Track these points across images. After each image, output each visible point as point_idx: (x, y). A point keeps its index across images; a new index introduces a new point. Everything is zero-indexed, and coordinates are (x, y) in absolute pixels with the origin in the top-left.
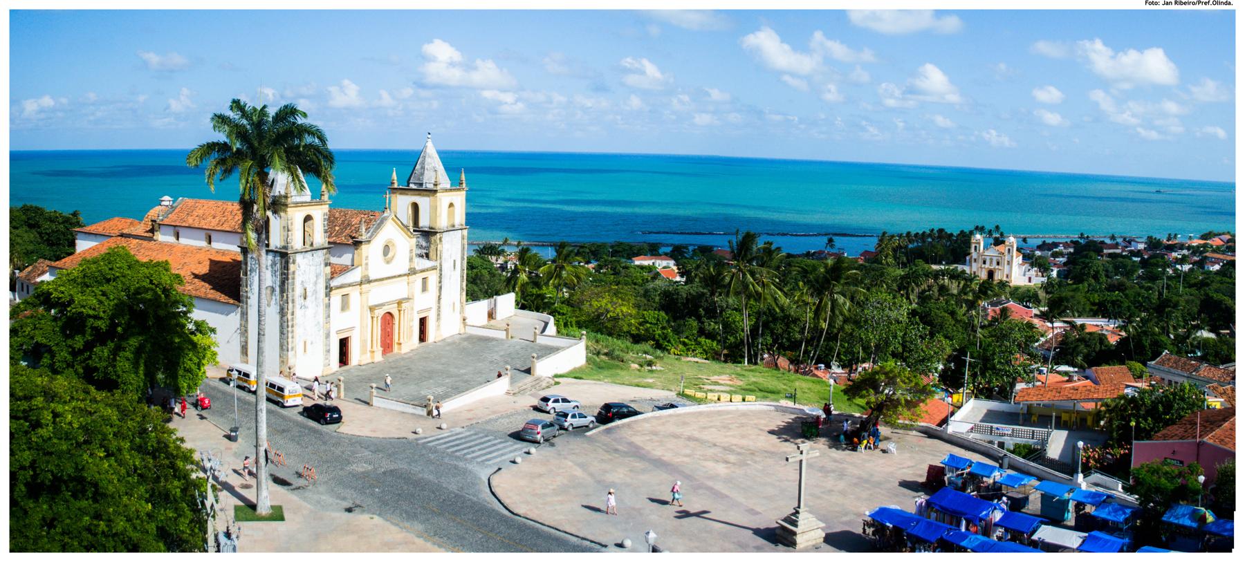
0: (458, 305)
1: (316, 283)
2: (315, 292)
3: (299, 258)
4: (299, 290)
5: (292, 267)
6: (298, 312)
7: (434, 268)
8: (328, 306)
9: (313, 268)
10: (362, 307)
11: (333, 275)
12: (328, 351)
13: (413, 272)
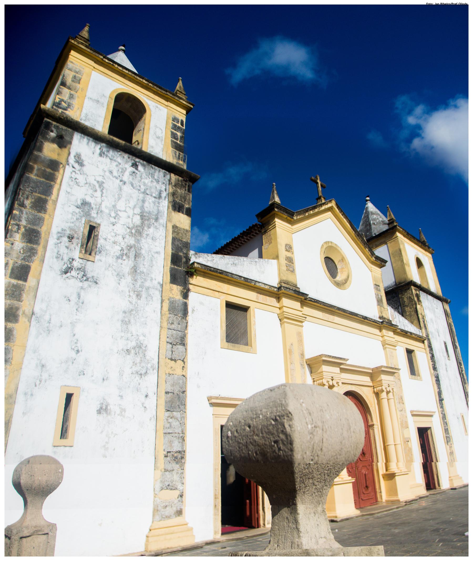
1: (138, 232)
2: (133, 252)
9: (127, 189)
10: (288, 352)
12: (178, 457)
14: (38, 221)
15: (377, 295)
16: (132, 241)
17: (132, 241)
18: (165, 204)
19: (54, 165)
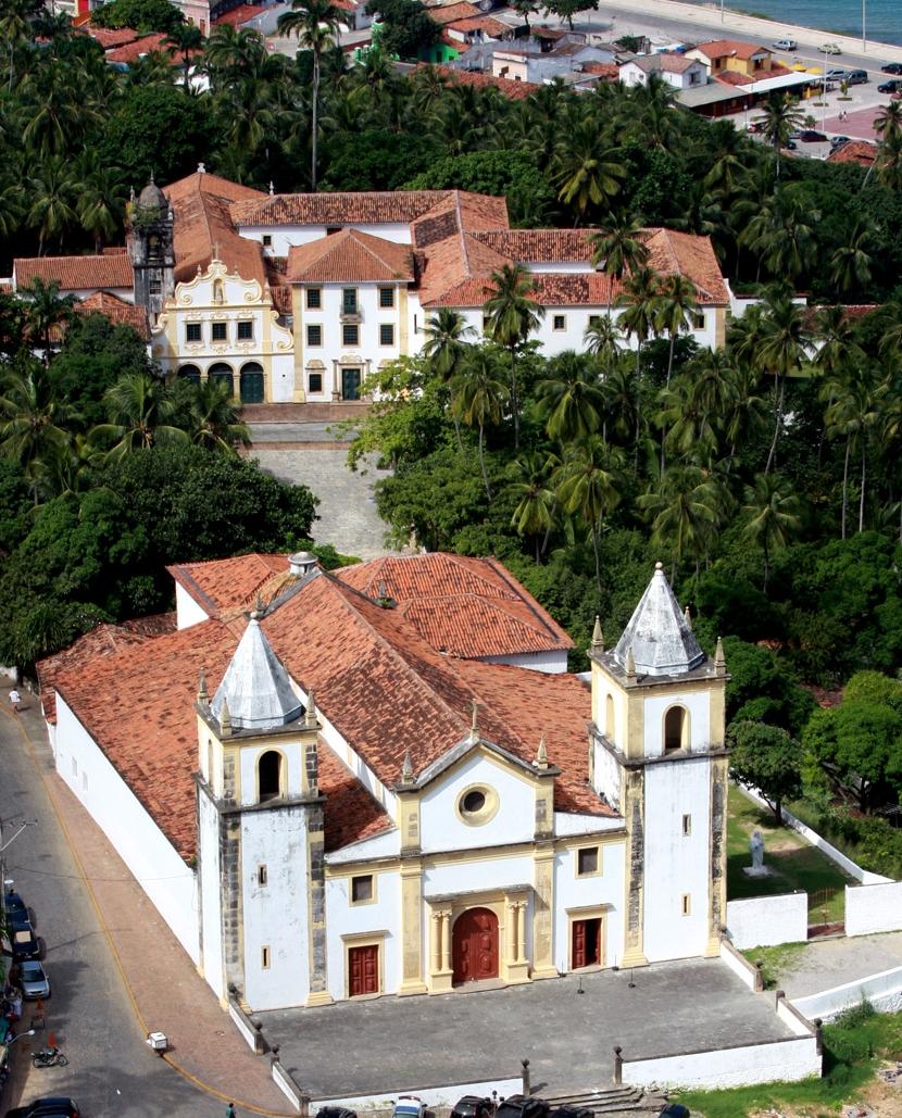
0: (700, 904)
1: (288, 859)
3: (245, 820)
4: (248, 870)
5: (231, 835)
6: (249, 903)
7: (618, 833)
8: (320, 895)
11: (331, 845)
13: (546, 840)
14: (235, 877)
15: (538, 812)
16: (284, 866)
17: (284, 866)
18: (304, 829)
19: (236, 843)
